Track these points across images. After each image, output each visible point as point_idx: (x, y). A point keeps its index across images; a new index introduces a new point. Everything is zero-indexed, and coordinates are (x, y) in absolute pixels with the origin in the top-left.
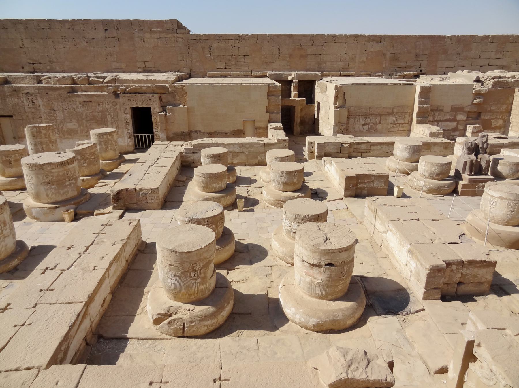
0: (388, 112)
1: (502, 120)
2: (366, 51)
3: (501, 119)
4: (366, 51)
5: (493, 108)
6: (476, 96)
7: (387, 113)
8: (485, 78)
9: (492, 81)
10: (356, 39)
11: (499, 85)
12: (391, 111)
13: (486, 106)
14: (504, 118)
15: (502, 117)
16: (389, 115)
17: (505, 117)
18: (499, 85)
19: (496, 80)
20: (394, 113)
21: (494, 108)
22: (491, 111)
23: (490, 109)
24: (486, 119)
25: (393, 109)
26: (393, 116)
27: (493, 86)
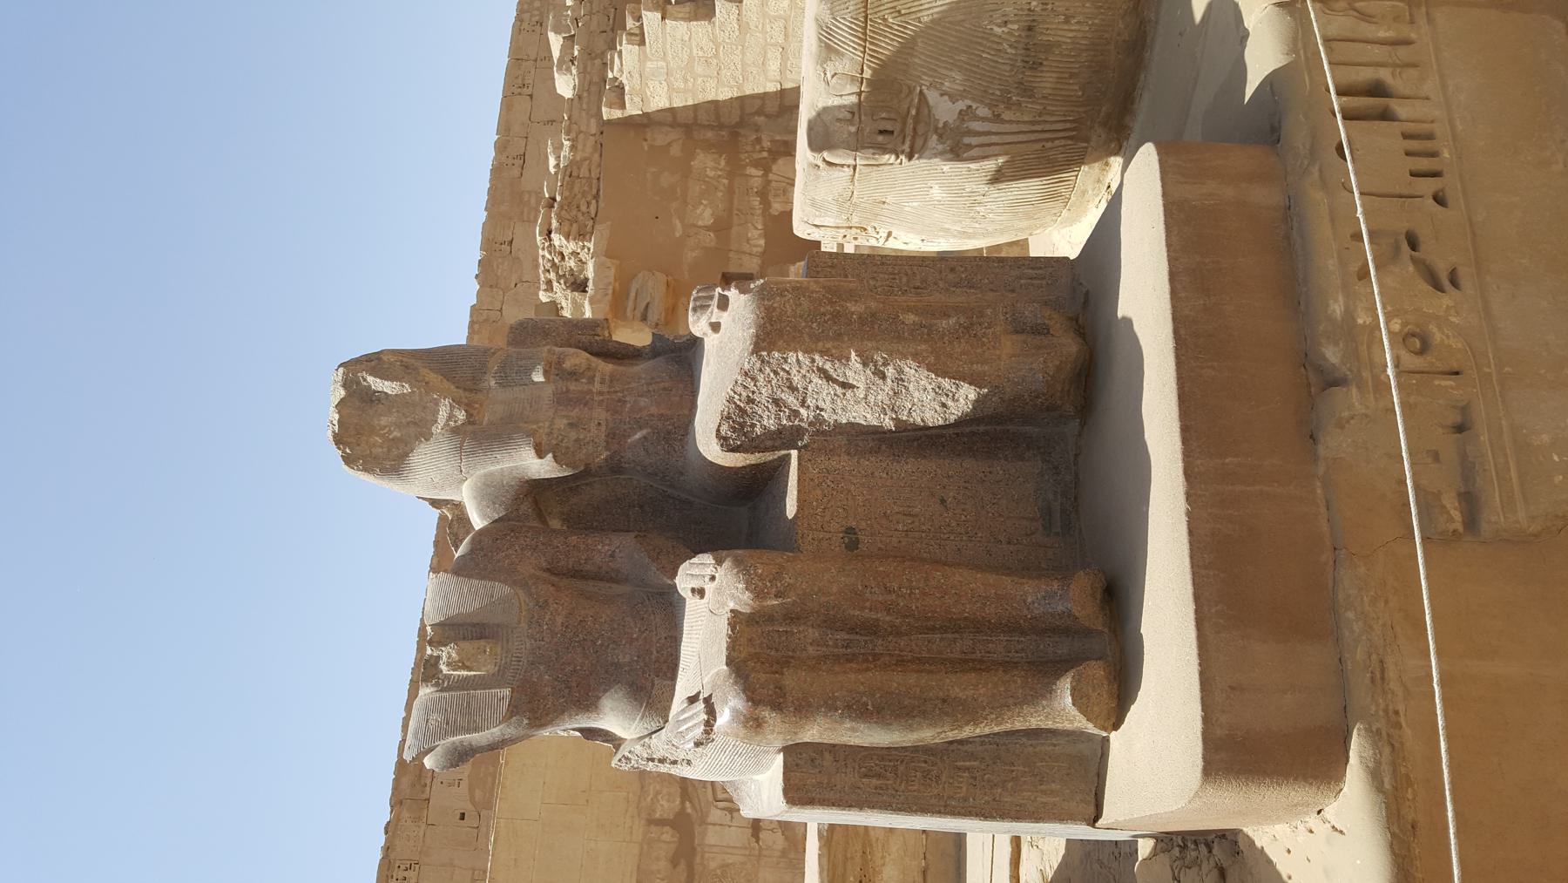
0: (674, 863)
1: (774, 160)
2: (462, 817)
3: (767, 170)
4: (462, 817)
5: (706, 216)
6: (629, 313)
7: (682, 866)
8: (552, 276)
9: (557, 239)
10: (401, 874)
11: (584, 208)
12: (668, 835)
13: (691, 255)
14: (765, 154)
15: (756, 164)
16: (692, 851)
17: (762, 150)
18: (584, 208)
19: (554, 224)
20: (682, 813)
21: (708, 212)
22: (722, 227)
23: (707, 228)
24: (762, 242)
25: (651, 822)
26: (703, 822)
27: (582, 235)
